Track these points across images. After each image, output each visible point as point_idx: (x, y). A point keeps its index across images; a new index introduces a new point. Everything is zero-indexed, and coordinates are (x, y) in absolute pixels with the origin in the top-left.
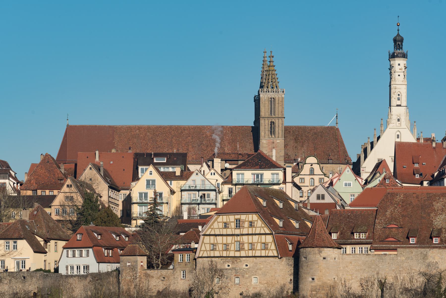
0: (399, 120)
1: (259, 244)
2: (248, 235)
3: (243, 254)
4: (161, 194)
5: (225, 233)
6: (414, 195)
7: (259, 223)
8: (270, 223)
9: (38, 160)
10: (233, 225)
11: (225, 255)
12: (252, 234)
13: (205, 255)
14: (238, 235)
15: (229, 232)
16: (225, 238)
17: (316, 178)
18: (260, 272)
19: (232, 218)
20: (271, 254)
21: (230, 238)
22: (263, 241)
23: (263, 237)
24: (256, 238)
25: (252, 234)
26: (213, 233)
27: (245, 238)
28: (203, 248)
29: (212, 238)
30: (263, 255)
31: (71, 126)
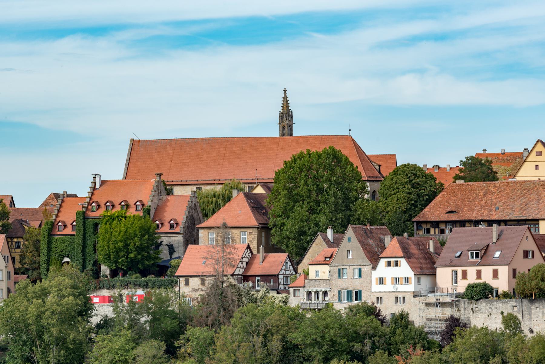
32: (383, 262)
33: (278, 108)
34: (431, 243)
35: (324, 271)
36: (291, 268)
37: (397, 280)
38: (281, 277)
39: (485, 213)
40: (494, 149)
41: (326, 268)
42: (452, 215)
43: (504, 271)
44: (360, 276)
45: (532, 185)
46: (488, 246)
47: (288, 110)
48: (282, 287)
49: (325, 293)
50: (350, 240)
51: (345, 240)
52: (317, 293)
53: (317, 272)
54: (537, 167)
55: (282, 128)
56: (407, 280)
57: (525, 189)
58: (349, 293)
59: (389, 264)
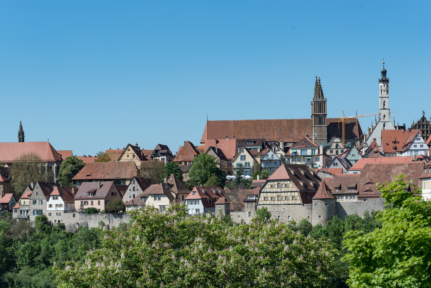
0: (384, 116)
1: (291, 198)
2: (285, 192)
3: (282, 202)
4: (249, 163)
5: (272, 191)
6: (382, 165)
7: (291, 185)
8: (297, 184)
9: (183, 145)
10: (276, 186)
11: (272, 203)
12: (287, 192)
13: (261, 203)
14: (279, 192)
15: (274, 190)
16: (272, 194)
17: (339, 151)
18: (291, 213)
19: (276, 183)
20: (297, 203)
21: (275, 194)
22: (293, 195)
23: (293, 193)
24: (289, 194)
25: (287, 192)
26: (265, 191)
27: (283, 194)
28: (260, 199)
29: (265, 194)
30: (293, 203)
31: (210, 121)
32: (51, 198)
33: (18, 129)
34: (73, 189)
35: (27, 201)
36: (15, 200)
37: (57, 205)
38: (10, 204)
39: (103, 176)
40: (114, 148)
41: (28, 200)
42: (88, 177)
43: (102, 202)
44: (42, 204)
45: (123, 164)
46: (96, 190)
47: (22, 130)
48: (10, 209)
49: (28, 211)
50: (37, 188)
51: (36, 188)
52: (24, 211)
53: (24, 202)
54: (128, 156)
55: (20, 139)
56: (61, 205)
57: (120, 165)
58: (37, 211)
59: (54, 199)
